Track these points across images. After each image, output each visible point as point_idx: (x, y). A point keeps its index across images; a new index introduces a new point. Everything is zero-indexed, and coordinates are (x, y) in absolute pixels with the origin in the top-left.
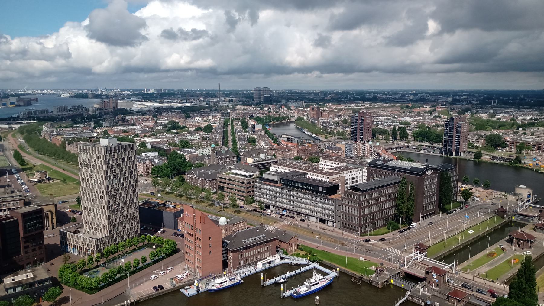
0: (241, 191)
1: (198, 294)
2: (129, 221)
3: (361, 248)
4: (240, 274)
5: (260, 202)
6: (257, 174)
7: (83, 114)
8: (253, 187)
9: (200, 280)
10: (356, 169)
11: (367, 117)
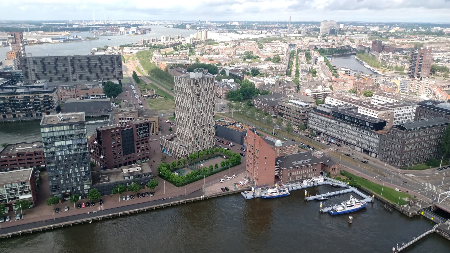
0: (297, 119)
1: (254, 199)
2: (207, 136)
3: (399, 180)
4: (288, 187)
5: (312, 130)
6: (313, 105)
8: (307, 115)
9: (257, 187)
10: (407, 107)
11: (427, 54)
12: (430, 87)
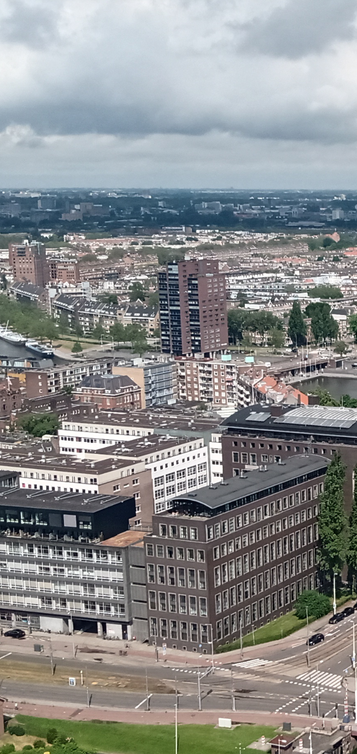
10: (187, 445)
12: (242, 378)
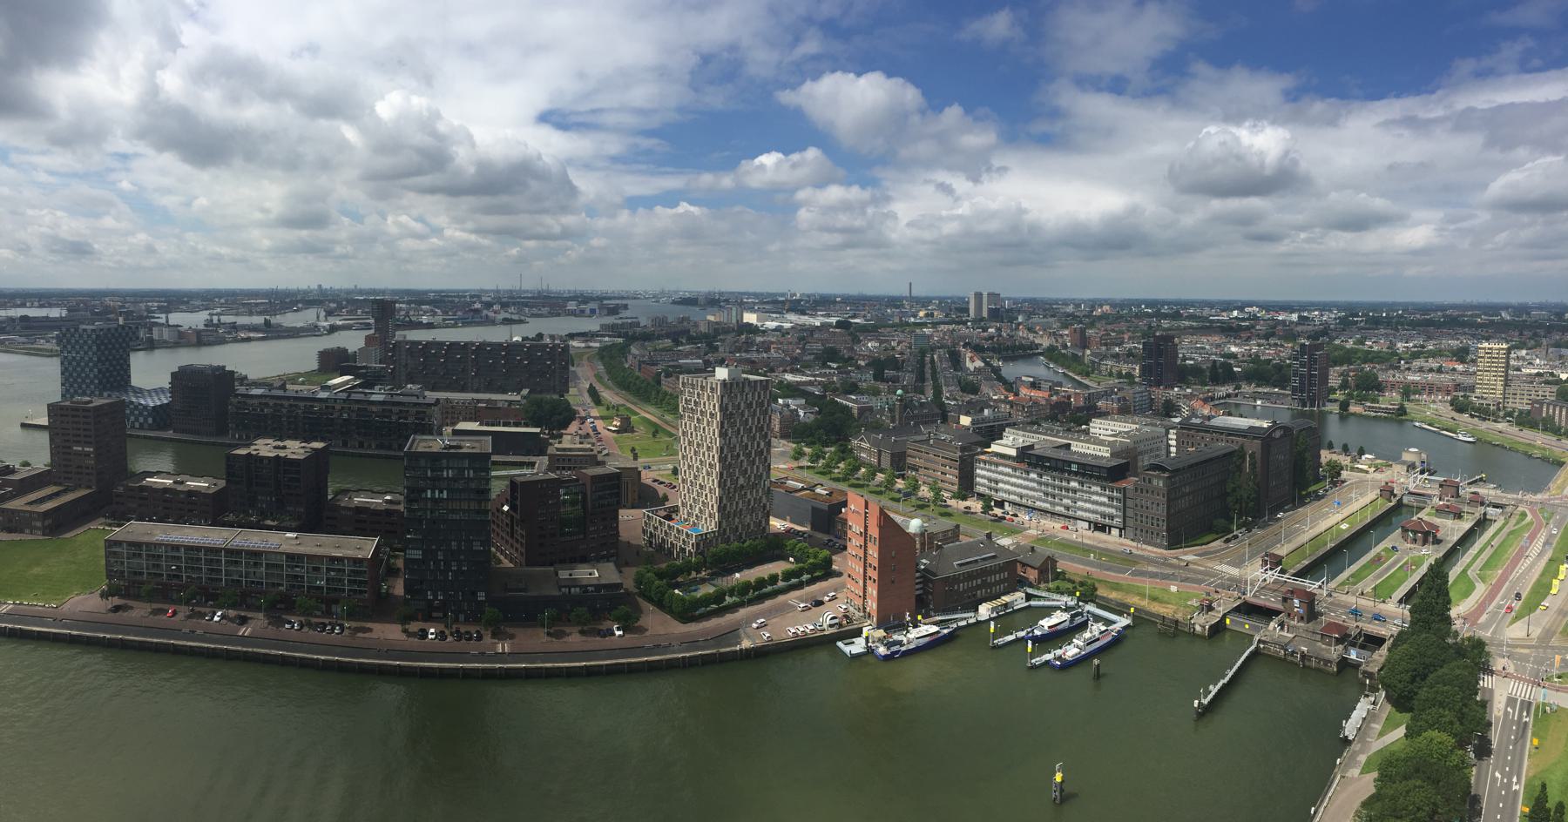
7: (689, 331)
